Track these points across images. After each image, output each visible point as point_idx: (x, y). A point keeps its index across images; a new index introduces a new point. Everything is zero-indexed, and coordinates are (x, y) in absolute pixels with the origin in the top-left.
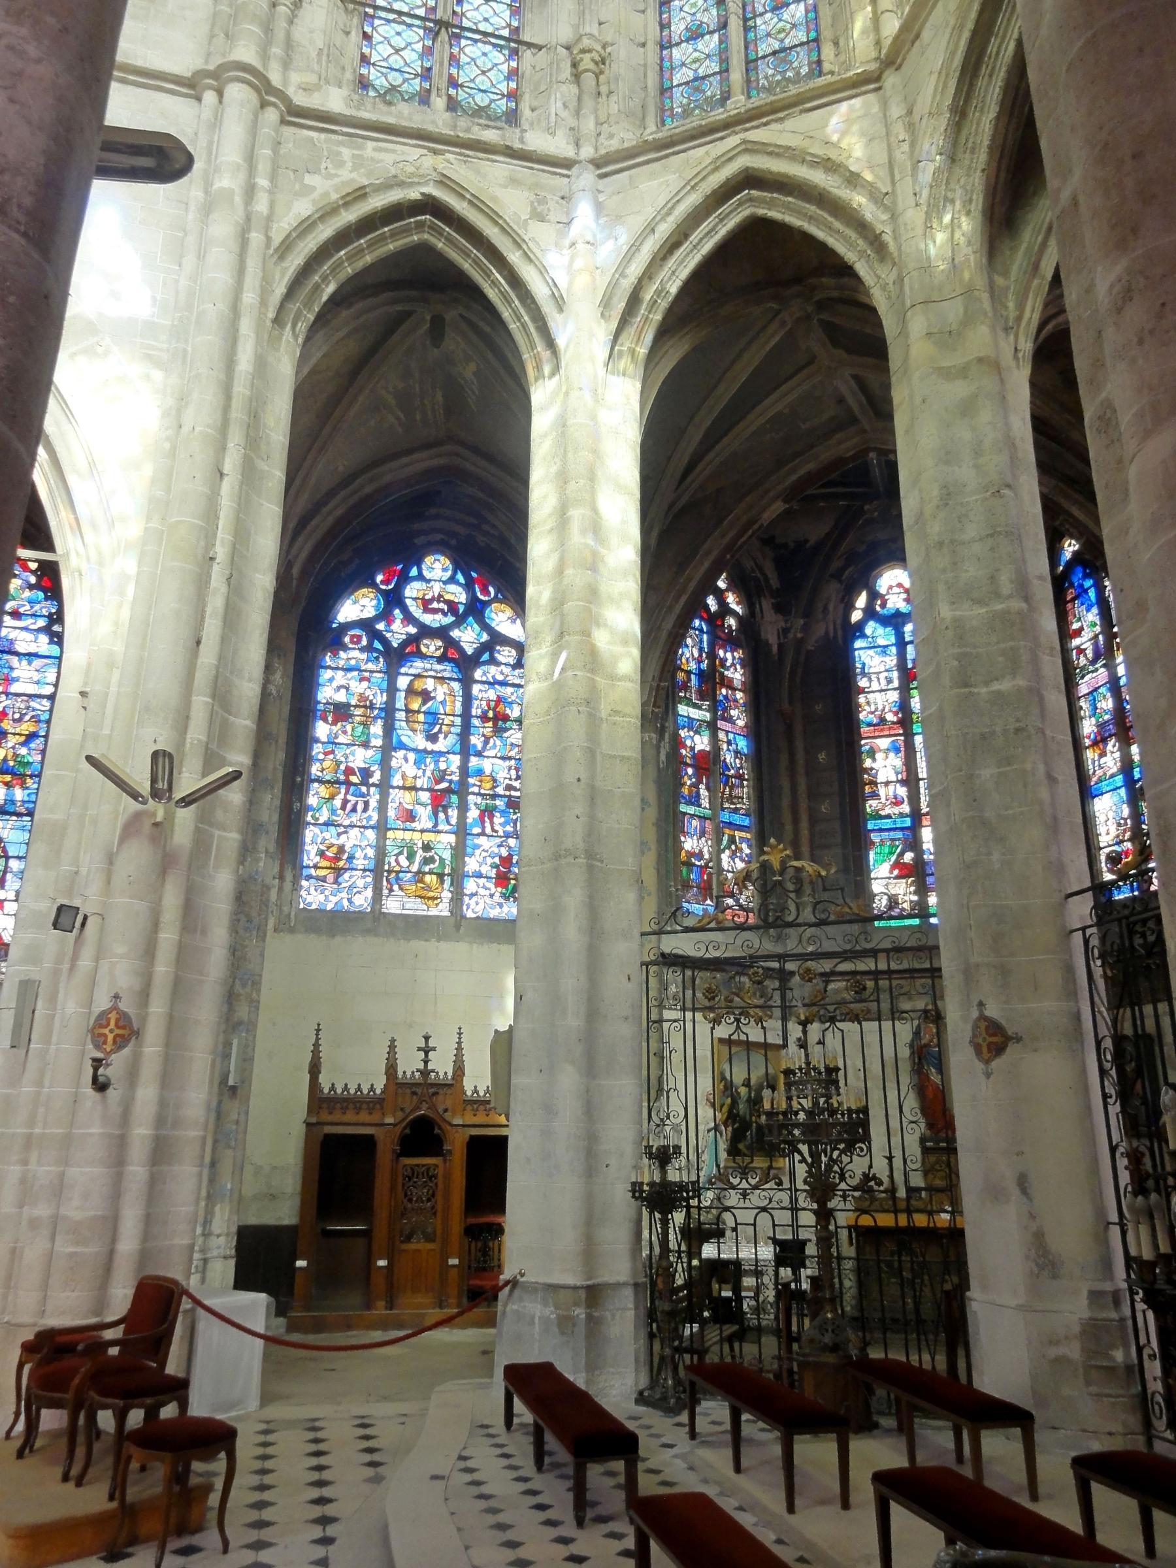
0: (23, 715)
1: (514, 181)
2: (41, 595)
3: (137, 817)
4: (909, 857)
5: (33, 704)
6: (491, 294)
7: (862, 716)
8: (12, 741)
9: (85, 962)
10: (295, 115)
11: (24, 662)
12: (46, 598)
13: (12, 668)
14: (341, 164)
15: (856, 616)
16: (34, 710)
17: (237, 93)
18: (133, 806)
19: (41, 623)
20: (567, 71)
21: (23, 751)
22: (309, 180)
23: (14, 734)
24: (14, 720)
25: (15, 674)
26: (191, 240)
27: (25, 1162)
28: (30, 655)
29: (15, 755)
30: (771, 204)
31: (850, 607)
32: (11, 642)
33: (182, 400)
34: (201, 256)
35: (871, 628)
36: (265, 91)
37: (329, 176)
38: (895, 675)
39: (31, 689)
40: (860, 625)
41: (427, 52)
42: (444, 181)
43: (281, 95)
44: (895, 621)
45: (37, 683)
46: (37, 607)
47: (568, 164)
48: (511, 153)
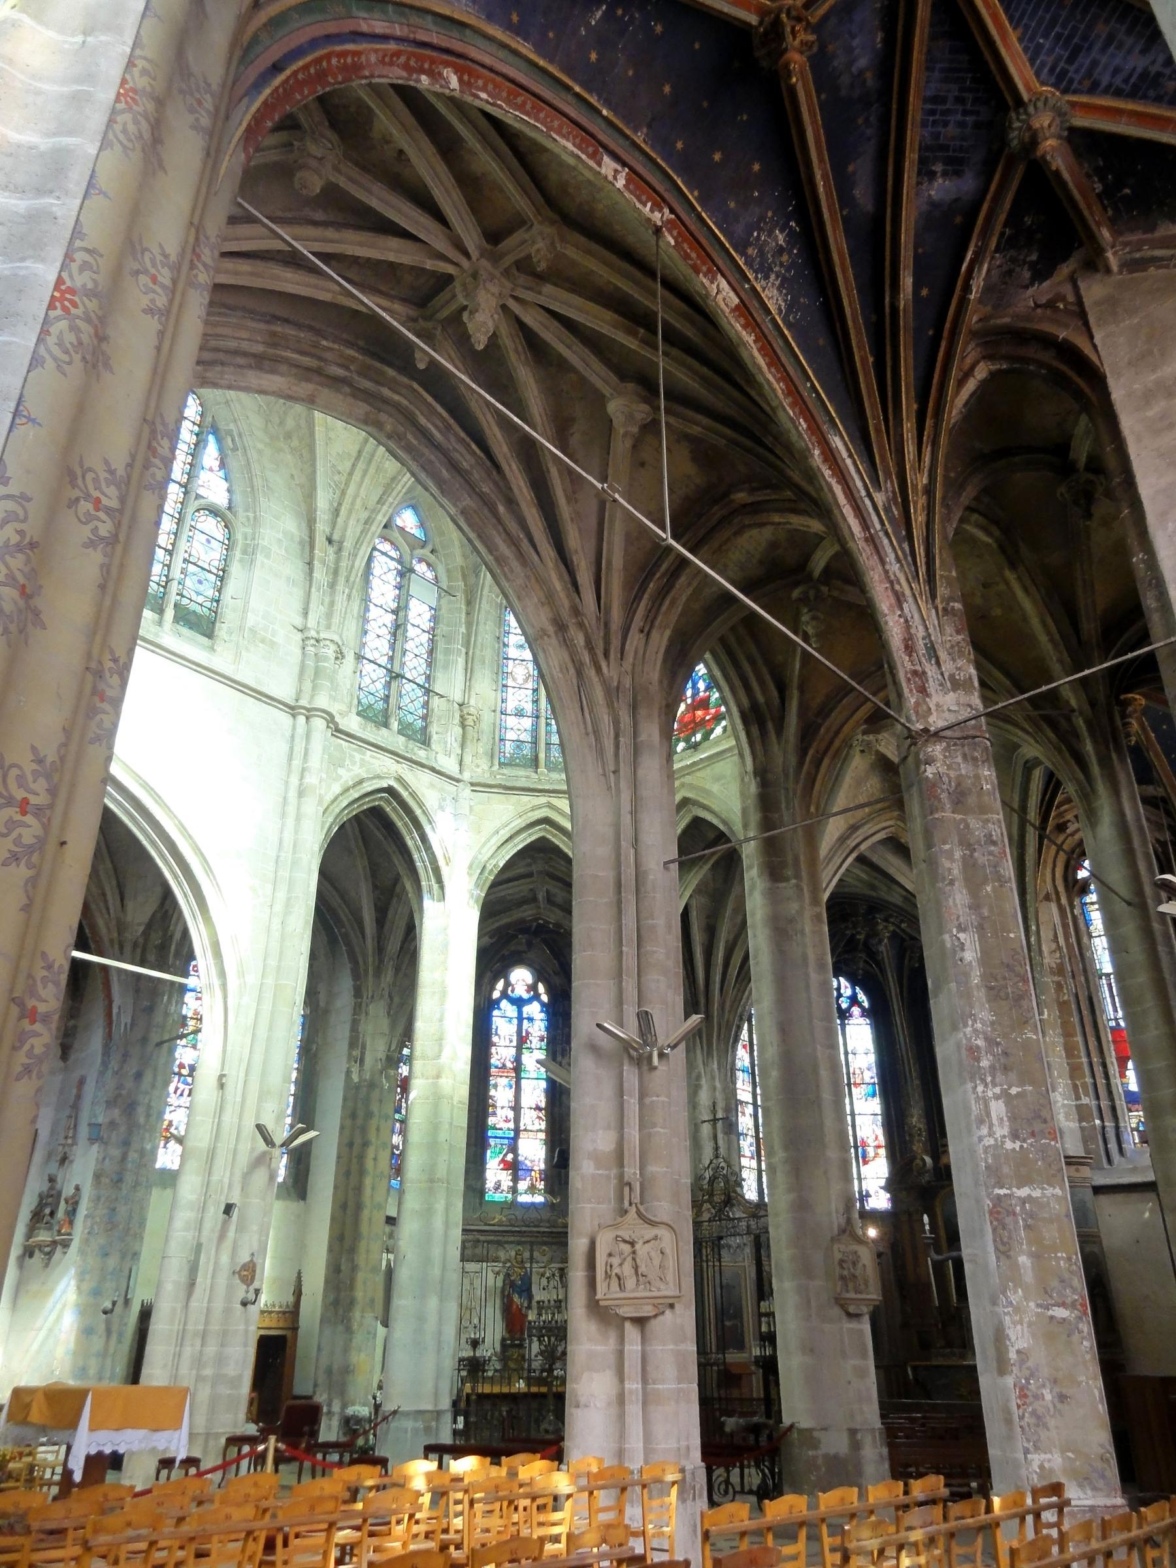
1: (432, 786)
3: (264, 1154)
4: (510, 1157)
6: (410, 843)
7: (493, 1061)
9: (231, 1234)
10: (338, 731)
14: (354, 763)
15: (496, 995)
17: (319, 724)
18: (262, 1146)
20: (457, 720)
22: (341, 771)
26: (291, 810)
30: (554, 836)
31: (493, 988)
35: (504, 1004)
36: (330, 719)
37: (349, 770)
38: (515, 1039)
40: (498, 1001)
41: (388, 685)
42: (399, 779)
43: (336, 724)
44: (519, 1003)
47: (458, 781)
48: (433, 770)
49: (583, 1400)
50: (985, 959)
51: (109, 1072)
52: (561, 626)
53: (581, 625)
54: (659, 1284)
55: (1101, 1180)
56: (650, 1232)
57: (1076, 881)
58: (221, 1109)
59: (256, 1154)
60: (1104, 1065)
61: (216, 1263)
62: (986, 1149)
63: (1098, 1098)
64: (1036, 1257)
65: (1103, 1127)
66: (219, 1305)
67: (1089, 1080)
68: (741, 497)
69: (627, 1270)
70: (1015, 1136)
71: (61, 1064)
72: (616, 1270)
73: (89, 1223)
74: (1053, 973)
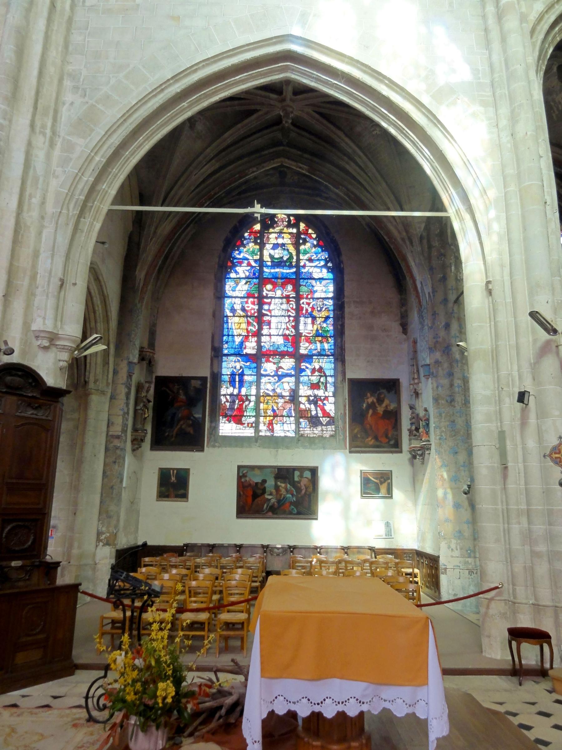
0: (321, 308)
2: (320, 250)
5: (325, 302)
8: (319, 321)
9: (532, 420)
11: (318, 283)
12: (322, 251)
13: (313, 286)
16: (326, 305)
18: (543, 335)
19: (322, 263)
21: (325, 325)
23: (319, 317)
24: (318, 311)
25: (315, 289)
26: (495, 35)
27: (519, 523)
28: (320, 279)
29: (321, 327)
32: (311, 274)
33: (513, 119)
34: (503, 40)
39: (323, 296)
45: (325, 292)
46: (319, 256)
51: (426, 327)
58: (494, 311)
59: (539, 344)
61: (524, 449)
66: (536, 486)
71: (405, 336)
73: (438, 432)
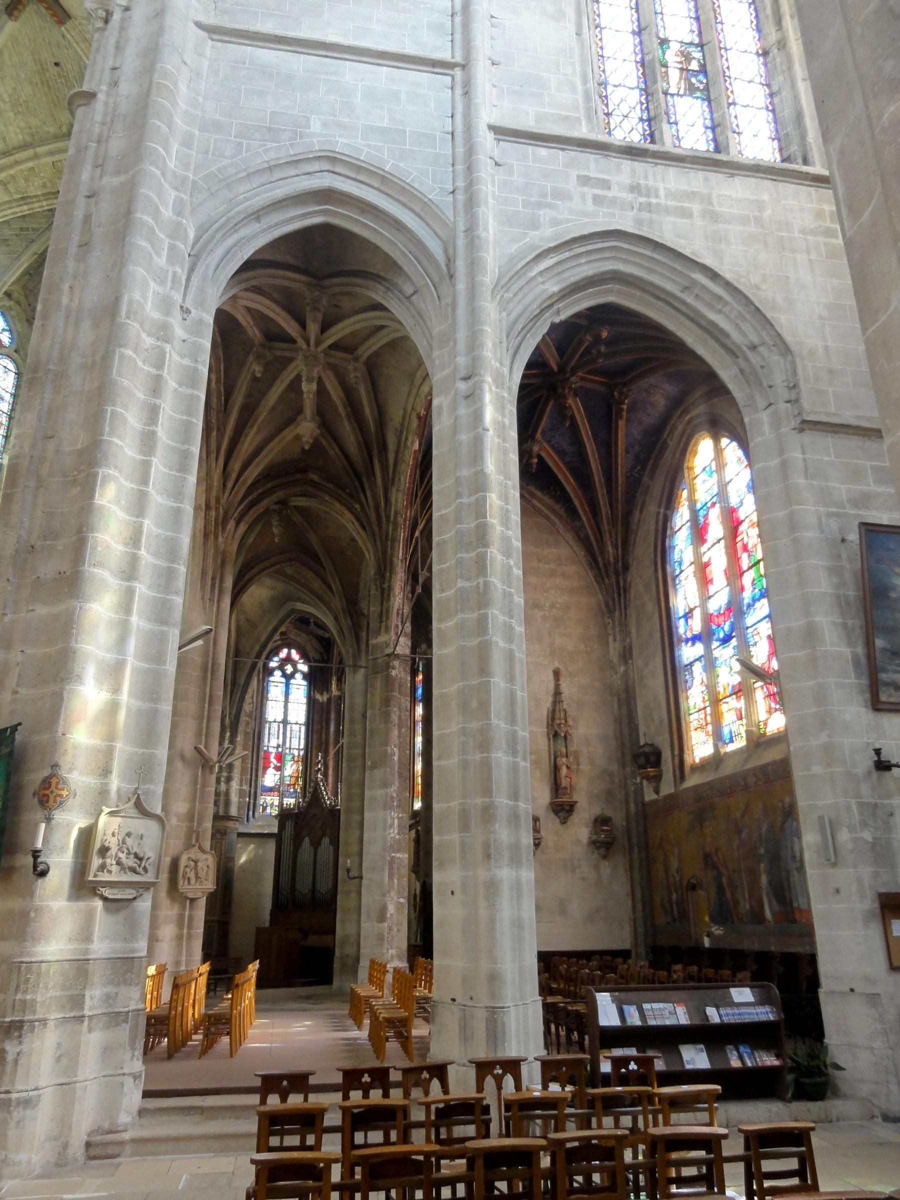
49: (160, 938)
50: (770, 883)
52: (208, 507)
53: (217, 509)
54: (205, 882)
55: (242, 829)
56: (204, 856)
57: (268, 669)
60: (257, 770)
62: (391, 838)
63: (250, 786)
64: (398, 879)
65: (249, 802)
67: (249, 777)
68: (315, 478)
69: (192, 875)
70: (399, 834)
72: (188, 875)
74: (246, 715)
